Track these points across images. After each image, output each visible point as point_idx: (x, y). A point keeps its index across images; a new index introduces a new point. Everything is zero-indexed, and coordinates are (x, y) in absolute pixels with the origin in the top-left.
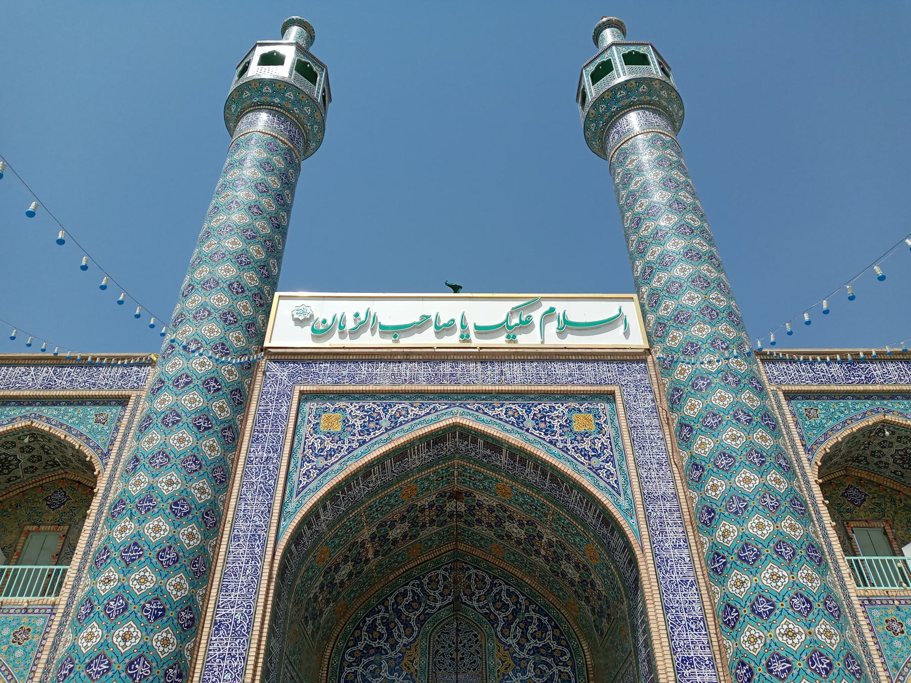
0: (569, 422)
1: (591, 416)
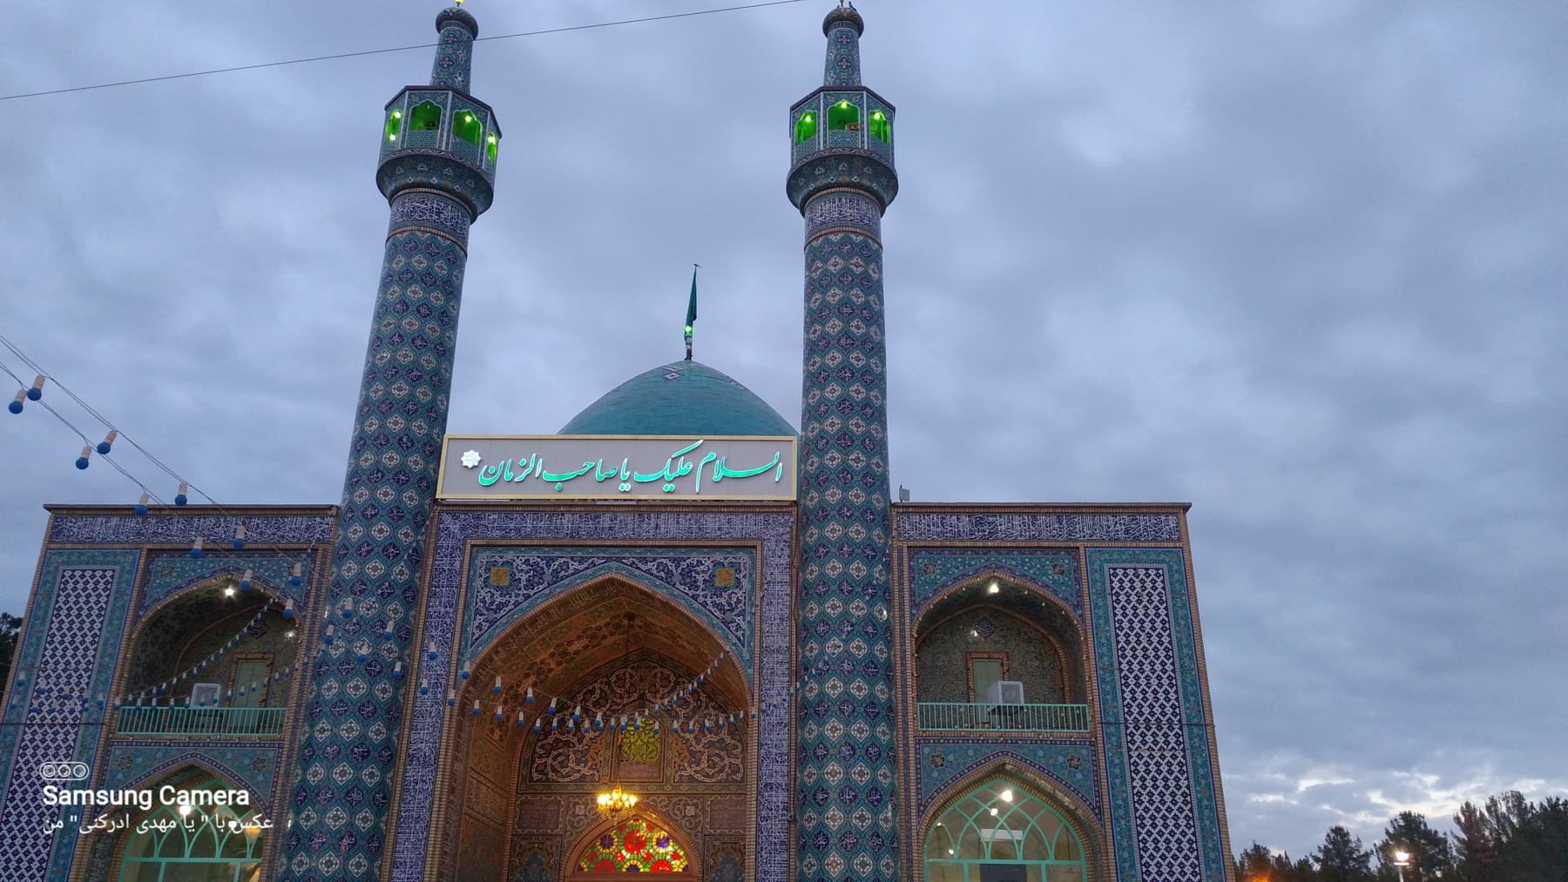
0: (712, 576)
1: (732, 571)
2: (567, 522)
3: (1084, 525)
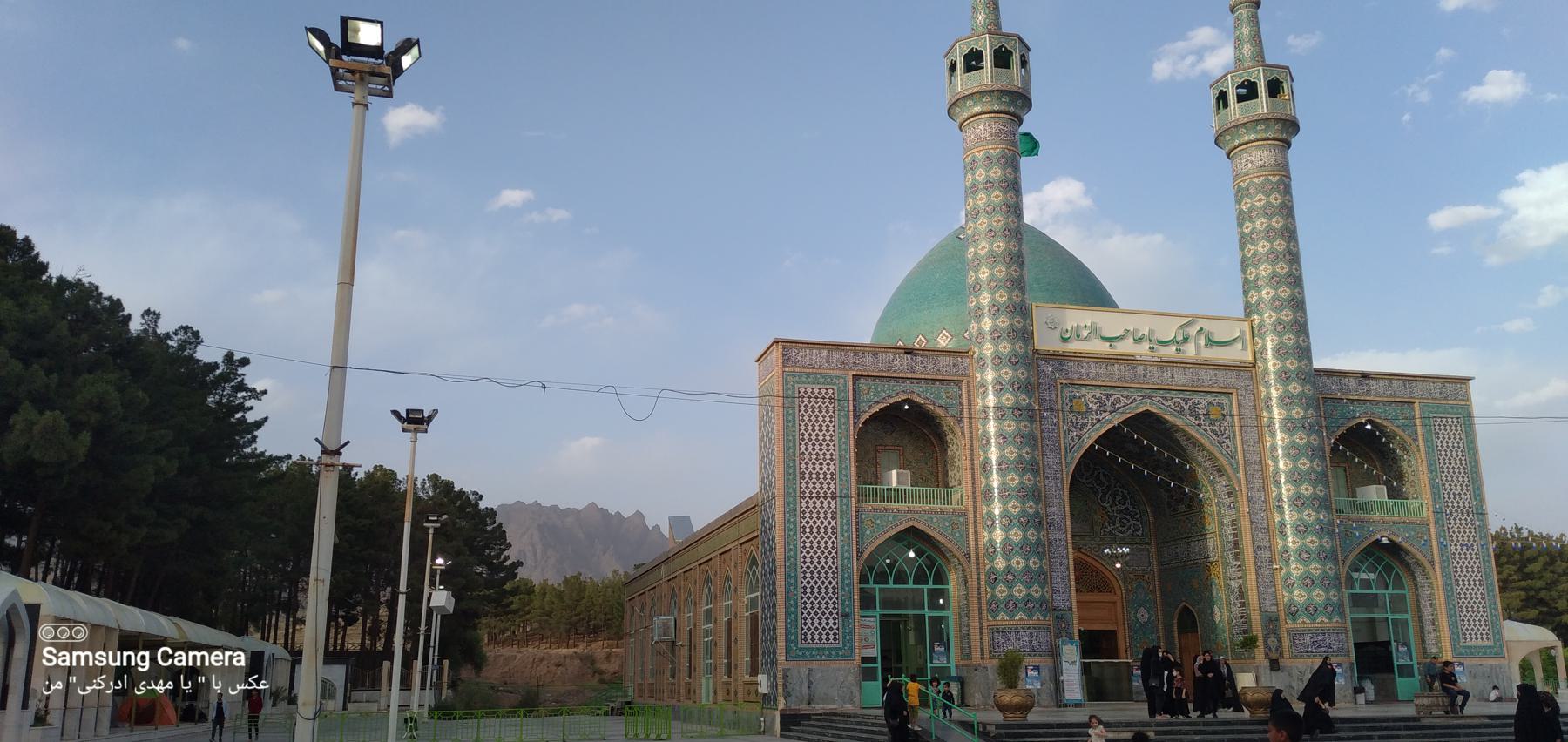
2: (1117, 370)
3: (1417, 386)
